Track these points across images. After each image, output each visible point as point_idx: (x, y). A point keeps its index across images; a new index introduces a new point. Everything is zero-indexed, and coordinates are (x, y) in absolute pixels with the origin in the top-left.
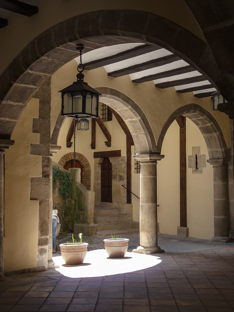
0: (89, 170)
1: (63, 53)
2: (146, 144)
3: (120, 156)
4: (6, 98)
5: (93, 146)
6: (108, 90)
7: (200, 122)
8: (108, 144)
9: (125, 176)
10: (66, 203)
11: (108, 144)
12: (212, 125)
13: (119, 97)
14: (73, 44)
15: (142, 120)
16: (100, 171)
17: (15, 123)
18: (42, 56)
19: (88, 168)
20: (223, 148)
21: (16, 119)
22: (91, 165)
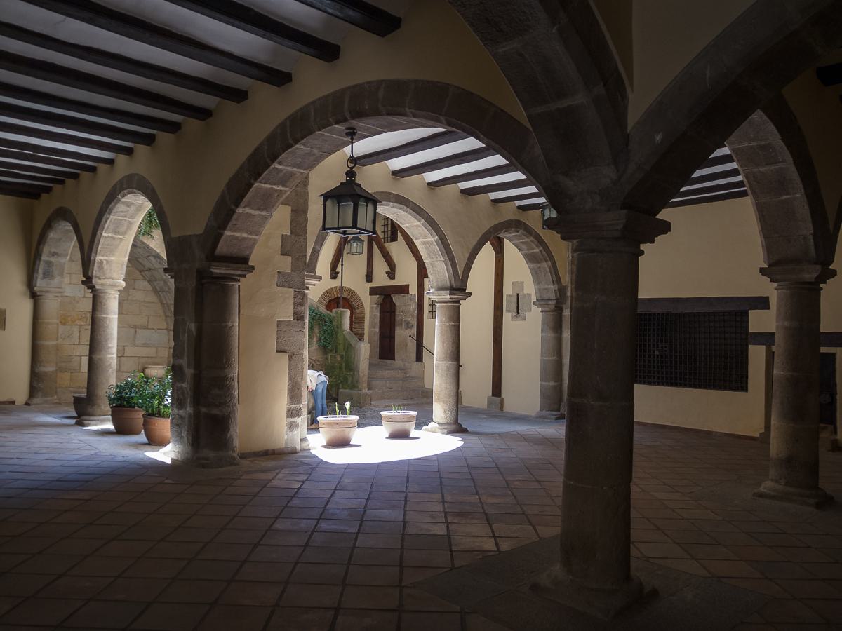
1: (326, 141)
2: (446, 276)
3: (408, 293)
4: (242, 204)
5: (369, 278)
7: (524, 247)
8: (391, 275)
9: (415, 323)
10: (327, 359)
11: (391, 275)
12: (541, 251)
14: (341, 127)
16: (378, 314)
17: (255, 240)
18: (296, 144)
20: (556, 285)
21: (257, 235)
22: (365, 305)
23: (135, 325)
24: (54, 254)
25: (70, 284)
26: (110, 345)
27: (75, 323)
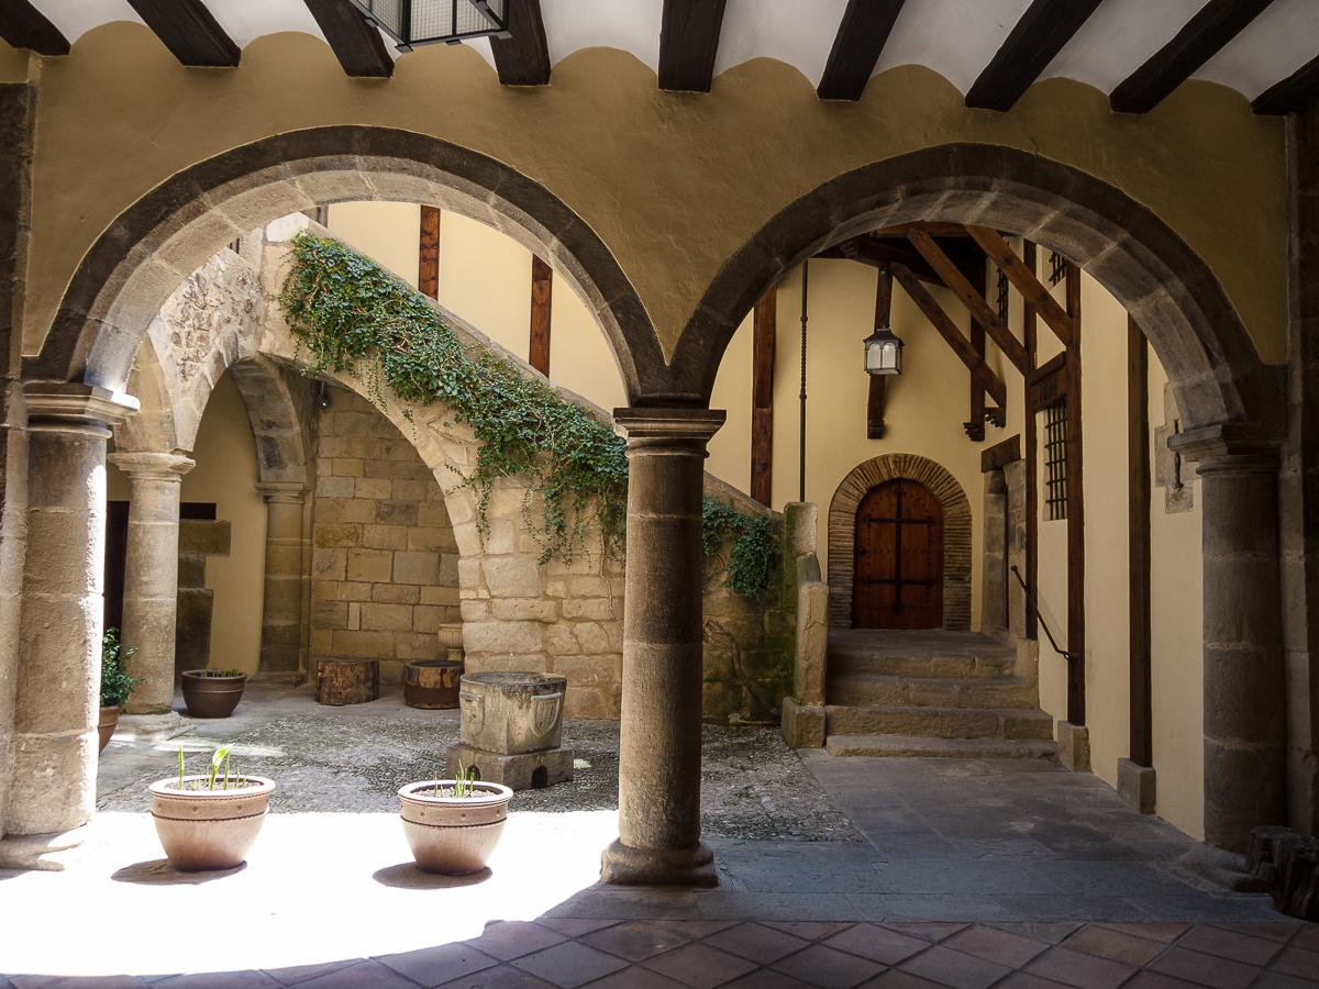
6: (357, 136)
10: (762, 623)
12: (1125, 245)
13: (424, 159)
15: (568, 252)
19: (958, 507)
23: (440, 547)
24: (270, 425)
25: (332, 475)
26: (145, 579)
27: (340, 543)
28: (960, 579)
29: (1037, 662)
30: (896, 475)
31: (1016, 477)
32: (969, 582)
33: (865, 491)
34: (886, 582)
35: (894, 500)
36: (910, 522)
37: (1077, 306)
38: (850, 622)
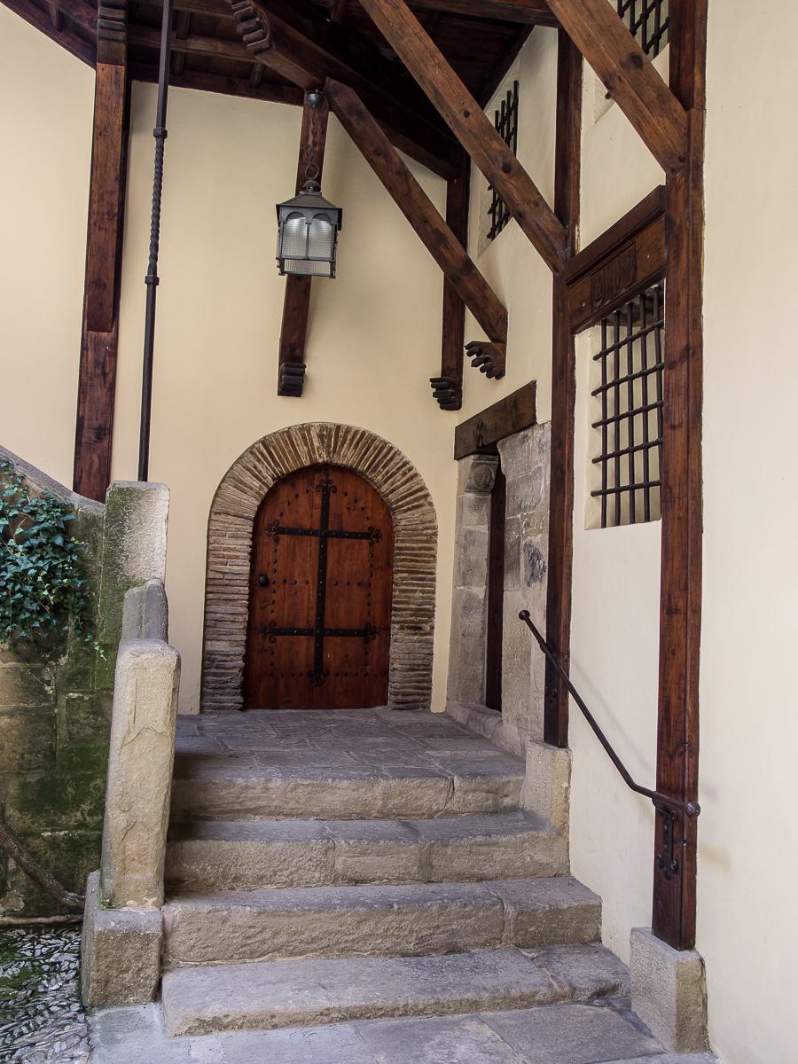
0: (423, 522)
19: (416, 514)
22: (435, 498)
28: (416, 628)
29: (567, 789)
30: (322, 457)
31: (528, 462)
32: (431, 633)
33: (271, 483)
34: (301, 632)
35: (318, 500)
36: (341, 535)
37: (698, 85)
38: (239, 699)
